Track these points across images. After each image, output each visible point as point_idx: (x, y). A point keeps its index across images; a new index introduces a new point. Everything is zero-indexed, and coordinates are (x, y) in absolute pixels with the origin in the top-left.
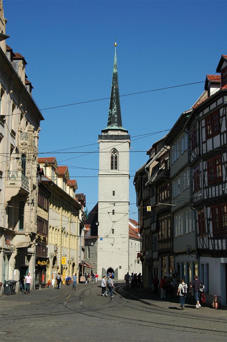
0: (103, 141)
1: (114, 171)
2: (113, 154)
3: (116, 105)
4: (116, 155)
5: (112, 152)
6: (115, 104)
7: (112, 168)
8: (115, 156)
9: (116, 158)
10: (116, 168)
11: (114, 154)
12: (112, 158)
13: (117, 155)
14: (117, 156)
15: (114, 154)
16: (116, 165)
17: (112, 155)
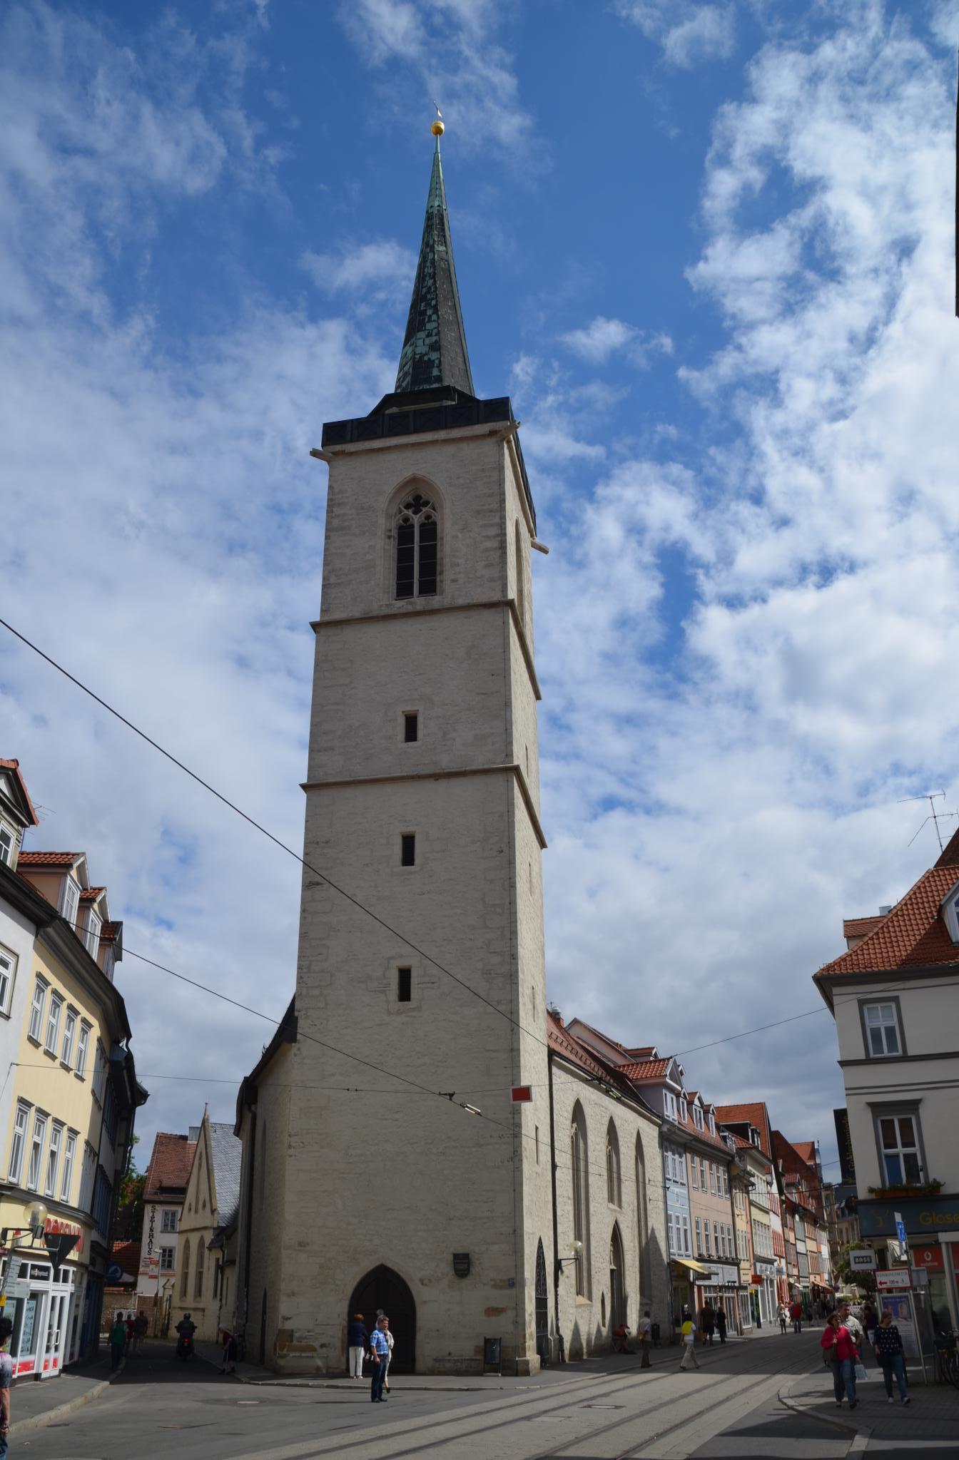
0: (350, 447)
1: (419, 602)
2: (410, 512)
4: (428, 517)
5: (408, 506)
6: (429, 312)
7: (403, 590)
8: (422, 525)
9: (430, 531)
11: (415, 513)
12: (404, 533)
13: (436, 517)
14: (435, 523)
17: (406, 520)
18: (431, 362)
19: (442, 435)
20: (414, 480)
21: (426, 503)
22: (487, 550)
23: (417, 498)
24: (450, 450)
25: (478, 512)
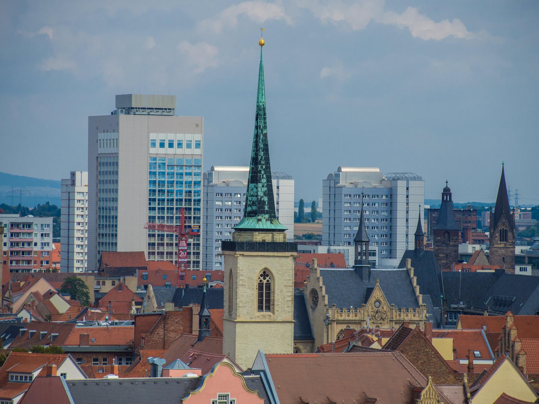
0: (246, 253)
2: (262, 278)
3: (265, 176)
4: (268, 281)
6: (263, 172)
7: (260, 308)
9: (268, 286)
10: (268, 308)
14: (270, 284)
15: (264, 279)
16: (268, 301)
17: (261, 281)
18: (264, 202)
19: (276, 254)
20: (265, 268)
21: (267, 276)
22: (288, 301)
23: (264, 272)
24: (277, 259)
25: (285, 286)
